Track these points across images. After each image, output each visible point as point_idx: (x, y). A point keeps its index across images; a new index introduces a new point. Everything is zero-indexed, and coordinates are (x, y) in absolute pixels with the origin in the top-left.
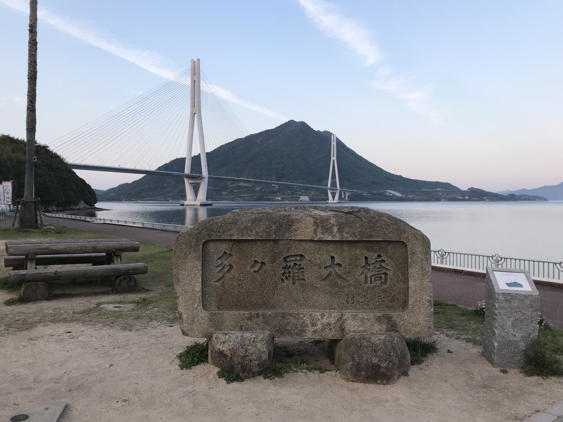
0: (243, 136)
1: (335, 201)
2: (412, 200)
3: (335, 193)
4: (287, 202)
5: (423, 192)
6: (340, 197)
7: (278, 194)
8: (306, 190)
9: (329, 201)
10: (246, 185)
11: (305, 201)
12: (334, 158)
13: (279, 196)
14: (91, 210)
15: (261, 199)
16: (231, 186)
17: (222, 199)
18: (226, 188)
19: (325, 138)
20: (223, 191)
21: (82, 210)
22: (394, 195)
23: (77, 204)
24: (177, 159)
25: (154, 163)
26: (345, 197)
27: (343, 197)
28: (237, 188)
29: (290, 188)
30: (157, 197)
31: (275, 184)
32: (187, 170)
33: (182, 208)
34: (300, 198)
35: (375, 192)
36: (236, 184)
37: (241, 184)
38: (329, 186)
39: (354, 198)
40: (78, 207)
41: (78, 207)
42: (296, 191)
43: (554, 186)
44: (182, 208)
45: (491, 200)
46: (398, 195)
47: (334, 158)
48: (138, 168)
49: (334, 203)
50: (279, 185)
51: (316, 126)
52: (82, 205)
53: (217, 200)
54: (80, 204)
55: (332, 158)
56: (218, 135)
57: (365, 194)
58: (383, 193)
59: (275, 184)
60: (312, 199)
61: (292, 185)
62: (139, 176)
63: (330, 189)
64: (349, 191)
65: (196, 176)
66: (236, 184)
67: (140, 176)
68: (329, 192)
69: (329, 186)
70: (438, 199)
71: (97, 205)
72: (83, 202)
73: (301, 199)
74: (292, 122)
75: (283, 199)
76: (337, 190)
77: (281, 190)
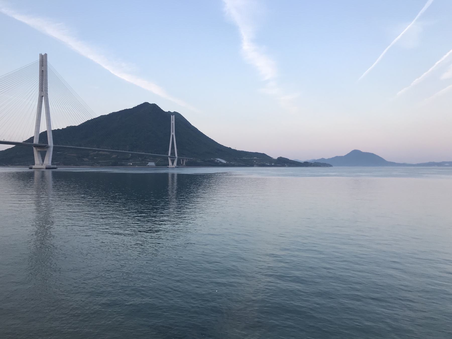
6: (179, 164)
7: (130, 160)
8: (153, 159)
9: (169, 166)
10: (108, 153)
12: (173, 133)
13: (131, 162)
15: (115, 164)
22: (221, 162)
26: (183, 163)
37: (101, 152)
38: (169, 155)
42: (146, 158)
43: (342, 157)
45: (289, 166)
46: (224, 161)
47: (173, 133)
49: (173, 168)
50: (132, 154)
53: (78, 165)
56: (66, 116)
60: (157, 165)
62: (14, 146)
63: (170, 157)
64: (186, 159)
69: (169, 155)
70: (252, 165)
74: (146, 104)
76: (175, 157)
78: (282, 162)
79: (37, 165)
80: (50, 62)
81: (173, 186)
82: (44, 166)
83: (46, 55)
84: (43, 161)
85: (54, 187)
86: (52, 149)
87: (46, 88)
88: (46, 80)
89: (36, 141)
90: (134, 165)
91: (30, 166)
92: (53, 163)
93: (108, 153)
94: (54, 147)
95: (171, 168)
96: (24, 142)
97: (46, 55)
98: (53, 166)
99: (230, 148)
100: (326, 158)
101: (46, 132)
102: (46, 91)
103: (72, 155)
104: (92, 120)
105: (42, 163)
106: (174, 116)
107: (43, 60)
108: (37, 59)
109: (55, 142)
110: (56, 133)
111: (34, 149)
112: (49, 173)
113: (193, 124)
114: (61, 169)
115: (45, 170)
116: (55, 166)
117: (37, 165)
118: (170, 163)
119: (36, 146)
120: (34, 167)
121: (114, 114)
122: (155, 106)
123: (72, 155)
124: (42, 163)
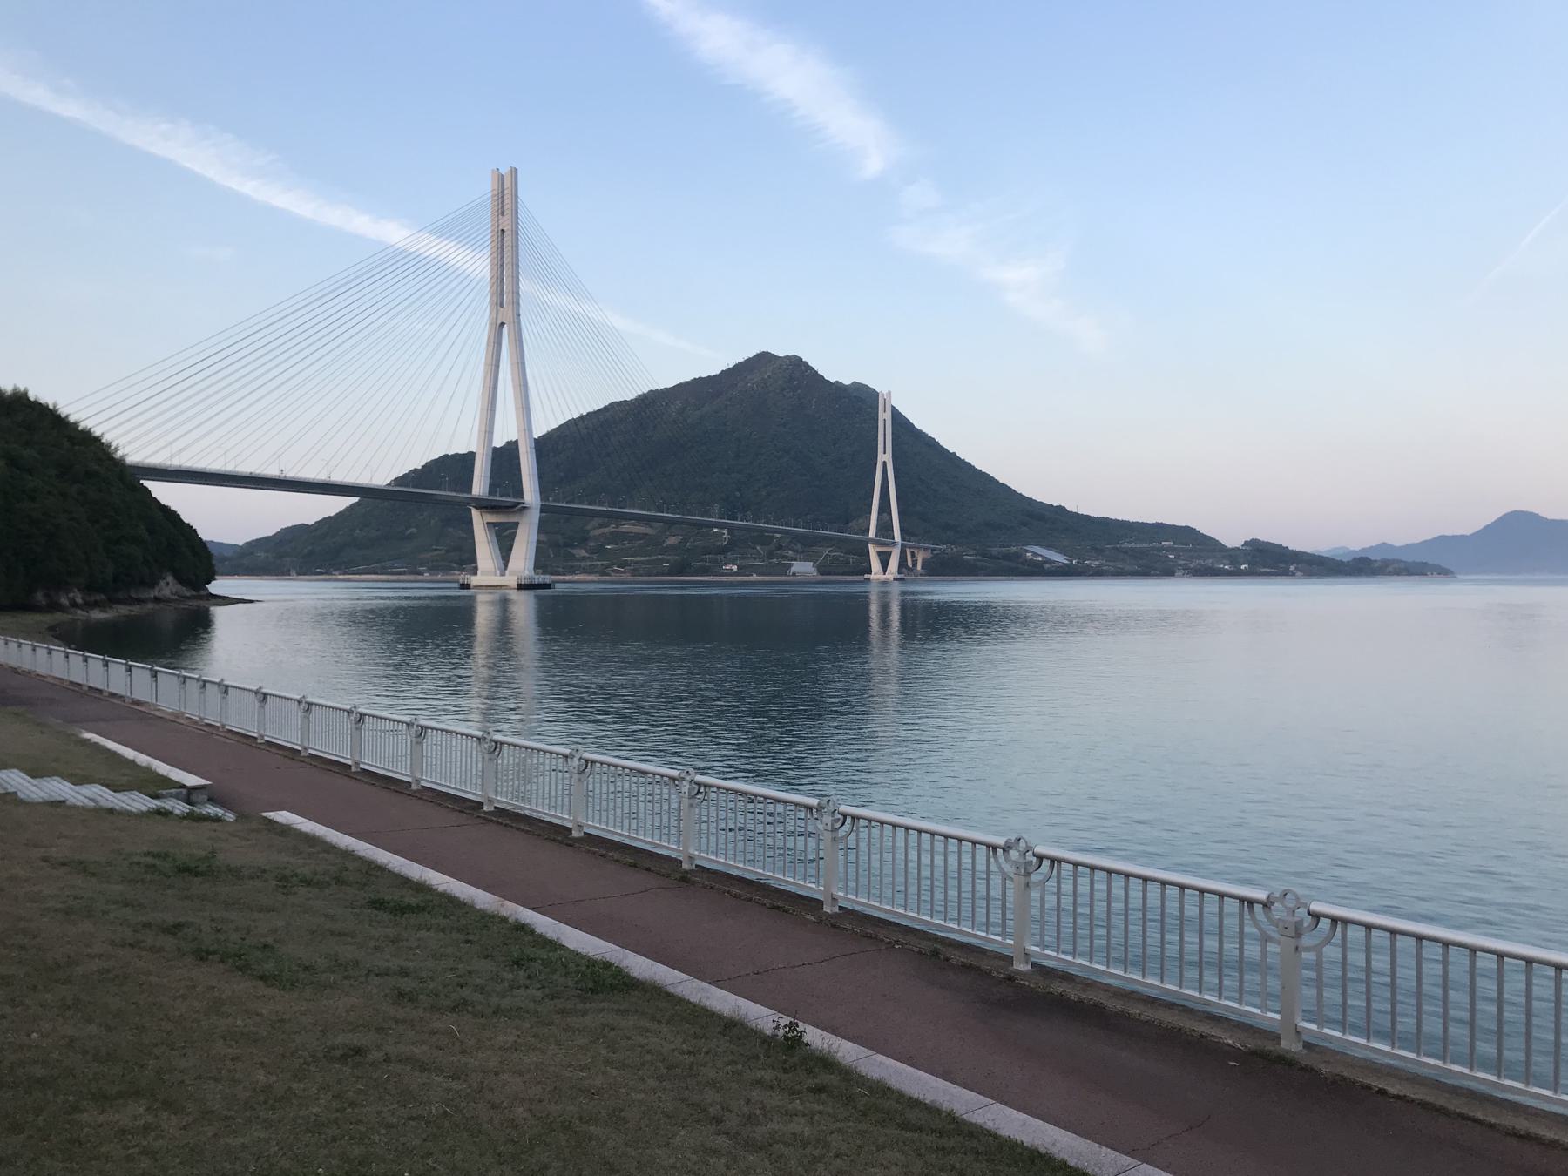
0: (630, 395)
2: (1098, 573)
3: (889, 554)
4: (755, 577)
5: (1125, 552)
8: (806, 546)
9: (872, 576)
11: (804, 574)
12: (885, 457)
13: (733, 561)
14: (195, 603)
15: (681, 569)
16: (597, 532)
17: (573, 571)
18: (584, 540)
19: (858, 404)
20: (573, 547)
21: (168, 600)
22: (1047, 561)
23: (153, 584)
24: (446, 456)
25: (382, 468)
26: (915, 564)
28: (616, 537)
29: (762, 538)
30: (388, 564)
34: (790, 566)
35: (995, 551)
36: (612, 528)
37: (626, 528)
38: (872, 534)
39: (941, 568)
40: (154, 593)
41: (154, 593)
42: (780, 547)
46: (1059, 558)
47: (885, 457)
48: (338, 477)
49: (885, 583)
50: (731, 529)
51: (836, 368)
52: (168, 587)
54: (162, 583)
58: (1018, 556)
59: (721, 526)
61: (768, 530)
62: (335, 505)
66: (612, 528)
67: (342, 503)
68: (873, 550)
69: (872, 534)
70: (1168, 572)
71: (216, 587)
72: (170, 578)
73: (793, 569)
74: (764, 358)
75: (743, 571)
76: (894, 544)
77: (738, 545)
78: (1266, 561)
79: (485, 573)
82: (511, 580)
84: (506, 565)
87: (516, 293)
89: (479, 487)
91: (463, 577)
92: (540, 565)
94: (543, 509)
97: (514, 172)
100: (1399, 540)
102: (516, 303)
105: (501, 570)
107: (505, 198)
108: (485, 188)
109: (544, 491)
111: (475, 514)
112: (524, 609)
115: (515, 595)
116: (548, 579)
117: (484, 573)
120: (475, 580)
122: (796, 364)
124: (501, 570)
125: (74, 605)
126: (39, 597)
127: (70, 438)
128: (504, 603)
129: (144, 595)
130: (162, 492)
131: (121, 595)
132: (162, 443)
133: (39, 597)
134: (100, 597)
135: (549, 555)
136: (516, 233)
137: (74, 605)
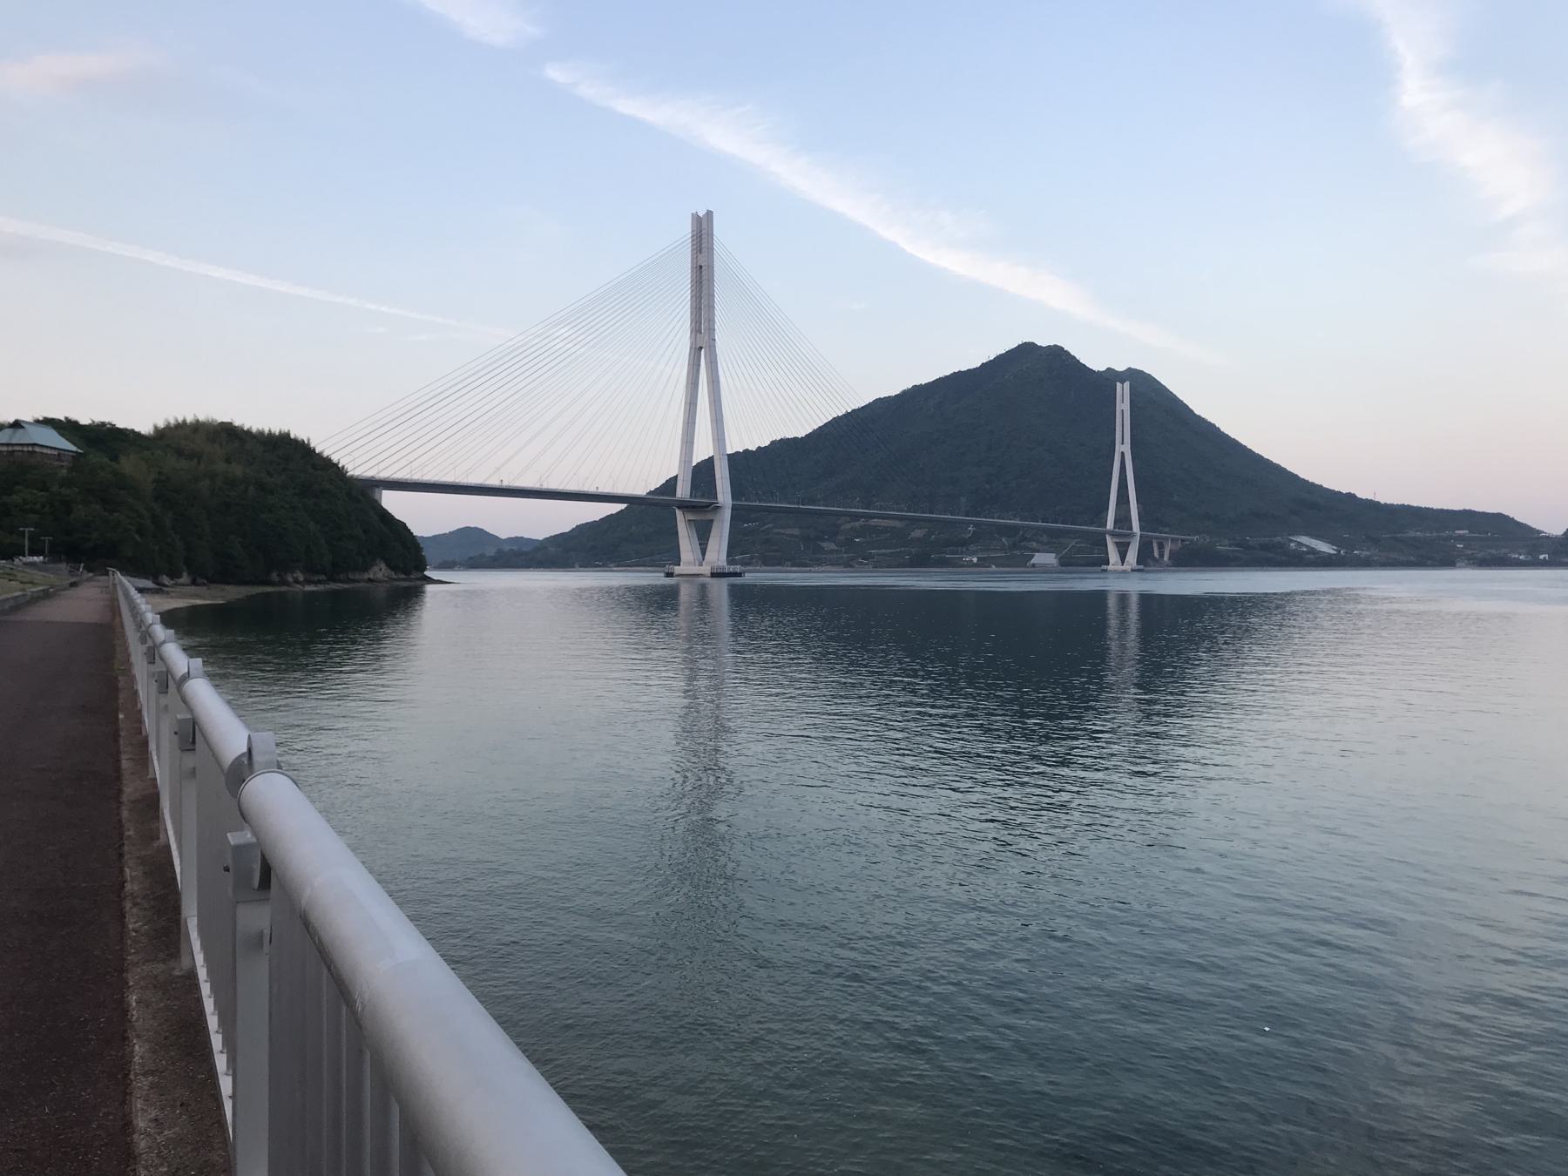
1: (1126, 567)
6: (1145, 558)
7: (972, 547)
8: (1052, 541)
9: (1110, 567)
12: (1123, 447)
13: (973, 553)
15: (920, 561)
16: (848, 526)
17: (819, 562)
22: (1312, 551)
23: (366, 569)
26: (1162, 555)
27: (1156, 554)
31: (970, 523)
32: (683, 491)
33: (669, 581)
37: (874, 522)
38: (1110, 525)
39: (1190, 559)
40: (366, 576)
41: (366, 576)
44: (669, 581)
46: (1324, 548)
47: (1123, 447)
49: (1124, 572)
50: (976, 524)
52: (380, 571)
54: (376, 568)
55: (1119, 448)
56: (772, 404)
57: (1223, 547)
63: (1113, 534)
65: (701, 506)
69: (1110, 525)
70: (1448, 562)
72: (383, 566)
76: (1133, 535)
80: (722, 234)
81: (1124, 641)
83: (709, 214)
84: (704, 554)
85: (737, 632)
86: (727, 514)
87: (711, 321)
88: (711, 296)
90: (983, 562)
91: (668, 568)
93: (897, 524)
94: (734, 508)
95: (1116, 572)
96: (651, 493)
97: (709, 214)
98: (732, 569)
99: (1351, 496)
101: (710, 461)
102: (711, 330)
103: (789, 531)
104: (847, 415)
105: (702, 556)
106: (1127, 384)
108: (686, 230)
109: (736, 493)
110: (740, 462)
111: (679, 513)
113: (1198, 410)
114: (757, 577)
116: (738, 568)
118: (1113, 555)
119: (685, 506)
120: (677, 570)
121: (917, 390)
123: (789, 531)
124: (702, 556)
125: (297, 581)
126: (274, 576)
127: (314, 467)
128: (703, 588)
129: (357, 577)
130: (391, 502)
131: (342, 577)
132: (404, 462)
133: (274, 576)
134: (323, 577)
135: (735, 547)
136: (711, 267)
137: (297, 581)
